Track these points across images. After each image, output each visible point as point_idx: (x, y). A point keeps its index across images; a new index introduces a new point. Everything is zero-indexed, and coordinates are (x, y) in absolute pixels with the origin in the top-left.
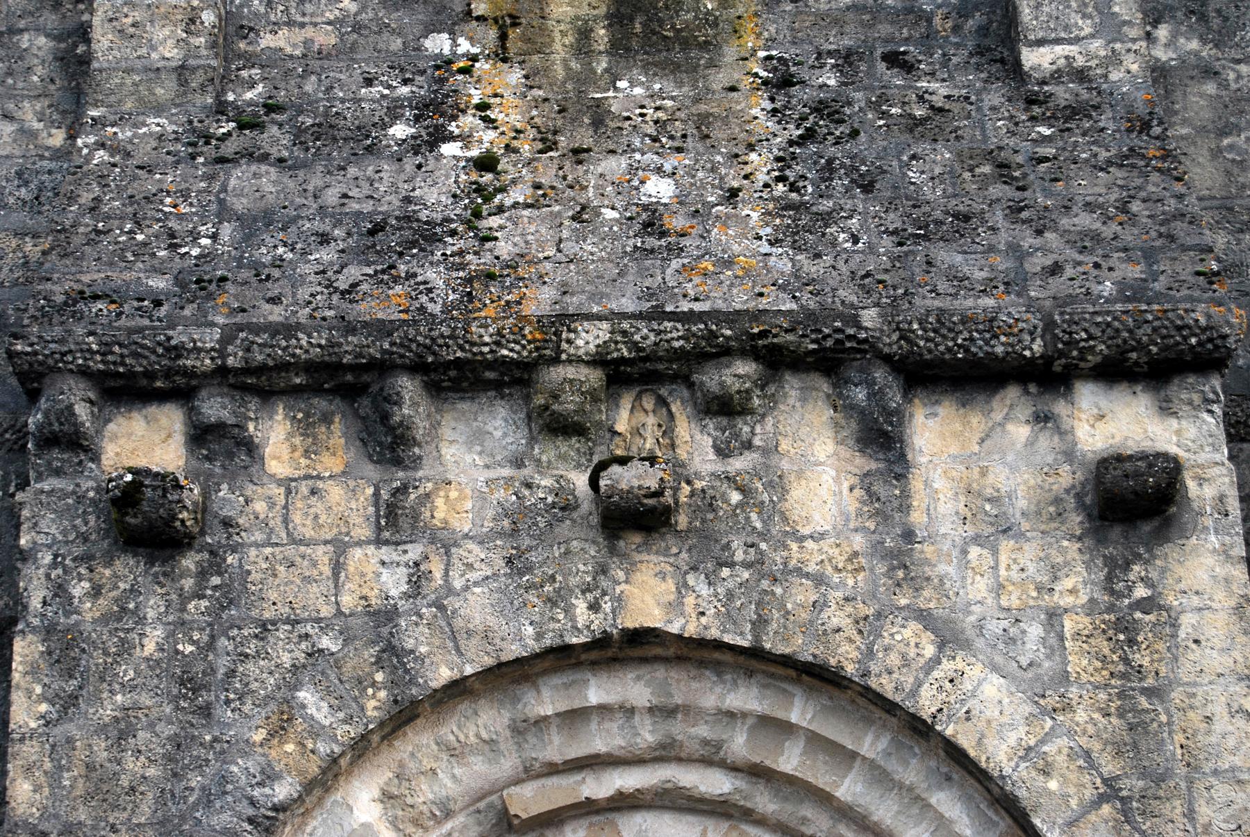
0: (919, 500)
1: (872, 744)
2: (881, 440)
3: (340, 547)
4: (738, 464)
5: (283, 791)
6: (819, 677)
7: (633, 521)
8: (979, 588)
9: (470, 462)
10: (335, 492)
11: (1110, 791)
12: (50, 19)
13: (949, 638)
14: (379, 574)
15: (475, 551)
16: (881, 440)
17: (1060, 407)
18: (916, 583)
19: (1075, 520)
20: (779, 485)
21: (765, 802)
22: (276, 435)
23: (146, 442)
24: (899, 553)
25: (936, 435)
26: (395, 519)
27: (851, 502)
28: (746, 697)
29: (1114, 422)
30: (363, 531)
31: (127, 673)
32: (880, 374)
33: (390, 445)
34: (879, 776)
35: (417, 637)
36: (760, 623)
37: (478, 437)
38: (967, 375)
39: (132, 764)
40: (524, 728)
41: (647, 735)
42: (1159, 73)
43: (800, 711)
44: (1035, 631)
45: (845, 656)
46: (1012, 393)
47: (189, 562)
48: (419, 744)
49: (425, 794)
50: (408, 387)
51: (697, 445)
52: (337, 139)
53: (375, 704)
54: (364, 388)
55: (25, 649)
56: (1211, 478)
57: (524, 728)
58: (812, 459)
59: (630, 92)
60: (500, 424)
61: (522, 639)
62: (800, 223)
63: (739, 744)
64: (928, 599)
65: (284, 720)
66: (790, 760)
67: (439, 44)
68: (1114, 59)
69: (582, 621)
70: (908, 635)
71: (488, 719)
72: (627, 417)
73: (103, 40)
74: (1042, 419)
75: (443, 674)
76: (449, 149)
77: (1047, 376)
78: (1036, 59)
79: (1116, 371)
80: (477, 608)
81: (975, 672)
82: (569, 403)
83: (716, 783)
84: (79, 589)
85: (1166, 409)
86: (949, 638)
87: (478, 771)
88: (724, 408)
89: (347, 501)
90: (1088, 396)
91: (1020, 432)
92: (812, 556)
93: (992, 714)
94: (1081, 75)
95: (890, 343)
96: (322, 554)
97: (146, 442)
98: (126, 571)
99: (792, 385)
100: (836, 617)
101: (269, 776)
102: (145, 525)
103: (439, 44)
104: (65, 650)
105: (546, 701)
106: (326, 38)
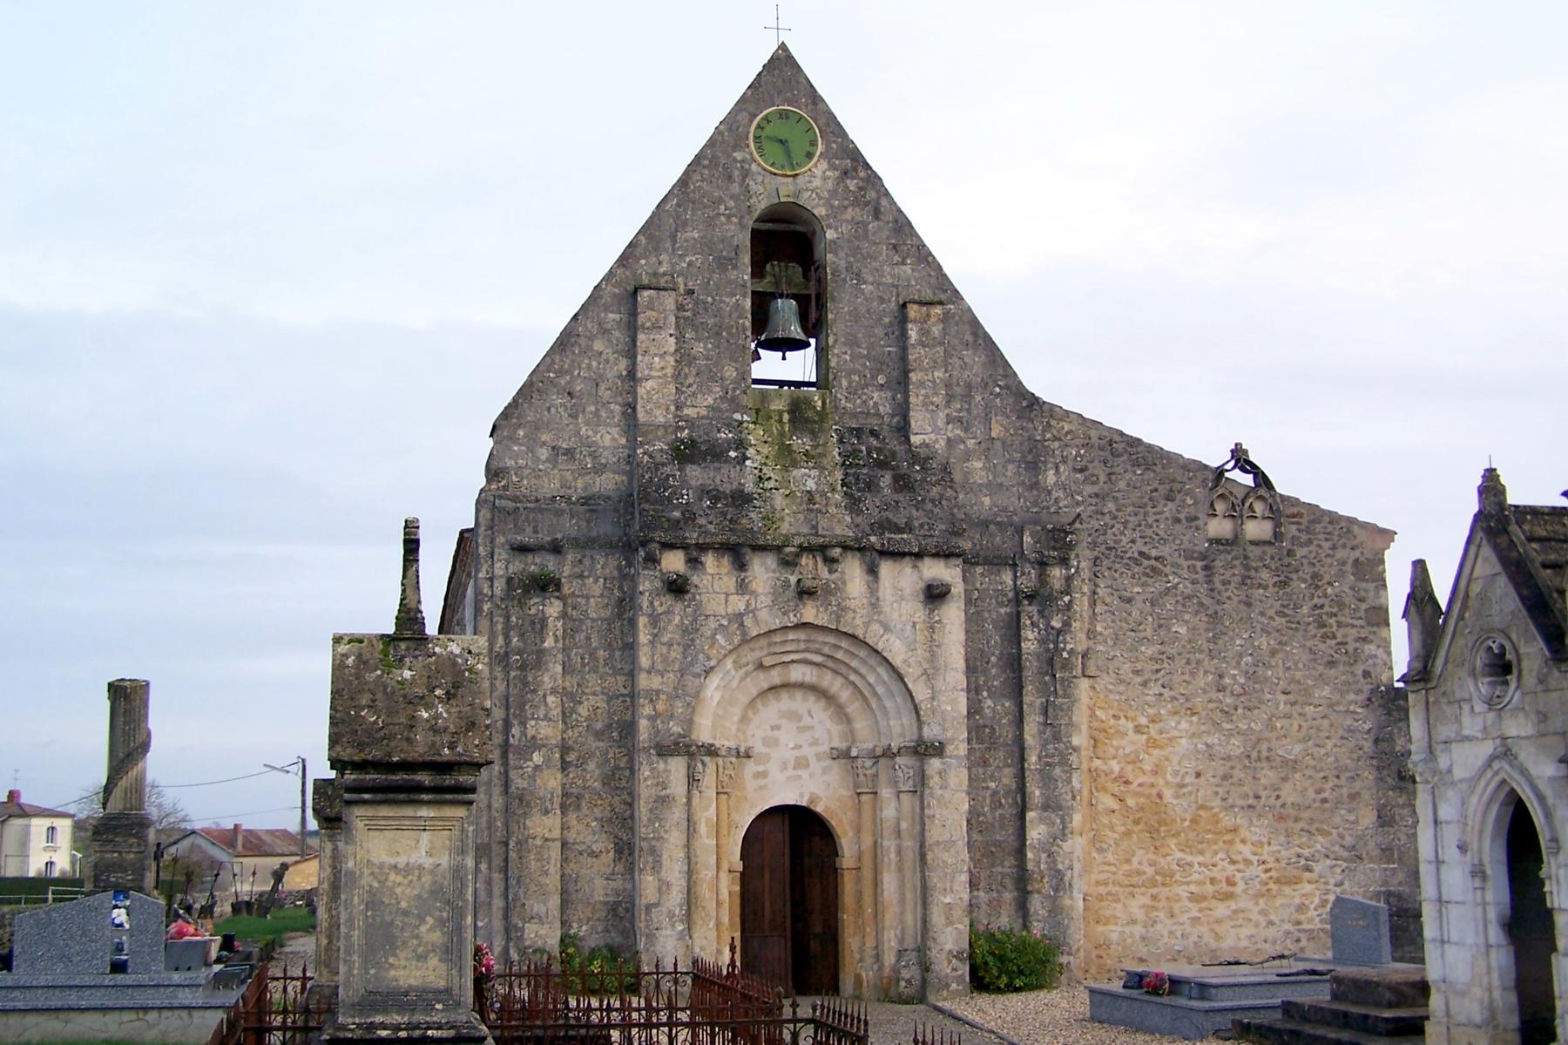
0: (881, 589)
1: (862, 653)
2: (873, 571)
3: (727, 595)
4: (836, 575)
5: (713, 663)
6: (853, 637)
7: (805, 593)
8: (895, 615)
9: (762, 571)
10: (726, 579)
11: (925, 672)
12: (620, 399)
13: (887, 628)
14: (738, 603)
15: (762, 598)
16: (873, 571)
17: (920, 564)
18: (880, 613)
19: (922, 597)
20: (844, 583)
21: (830, 664)
22: (709, 560)
23: (674, 562)
24: (875, 605)
25: (886, 568)
26: (742, 587)
27: (864, 588)
28: (831, 639)
29: (935, 570)
30: (733, 590)
31: (671, 628)
32: (875, 555)
33: (741, 565)
34: (863, 662)
35: (748, 621)
36: (838, 622)
37: (764, 564)
38: (897, 555)
39: (673, 654)
40: (770, 644)
41: (802, 646)
42: (949, 440)
43: (844, 644)
44: (909, 628)
45: (859, 633)
46: (907, 559)
47: (687, 597)
48: (744, 650)
49: (744, 661)
50: (748, 550)
51: (824, 572)
52: (715, 454)
53: (737, 640)
54: (737, 552)
55: (642, 621)
56: (958, 588)
57: (770, 644)
58: (853, 572)
59: (800, 443)
60: (771, 560)
61: (777, 624)
62: (853, 505)
63: (826, 650)
64: (882, 618)
65: (714, 642)
66: (839, 655)
67: (737, 416)
68: (936, 441)
69: (793, 619)
70: (876, 628)
71: (763, 642)
72: (805, 560)
73: (641, 416)
74: (915, 567)
75: (755, 633)
76: (748, 463)
77: (919, 556)
78: (915, 440)
79: (936, 555)
80: (763, 615)
81: (893, 639)
82: (789, 559)
83: (818, 659)
84: (656, 603)
85: (947, 567)
86: (887, 628)
87: (758, 654)
88: (831, 562)
89: (730, 582)
90: (927, 561)
91: (908, 570)
92: (852, 604)
93: (896, 650)
94: (927, 446)
95: (878, 547)
96: (723, 597)
97: (674, 562)
98: (668, 600)
99: (849, 554)
100: (858, 622)
101: (709, 659)
102: (677, 587)
103: (737, 416)
104: (654, 620)
105: (778, 638)
106: (704, 412)
